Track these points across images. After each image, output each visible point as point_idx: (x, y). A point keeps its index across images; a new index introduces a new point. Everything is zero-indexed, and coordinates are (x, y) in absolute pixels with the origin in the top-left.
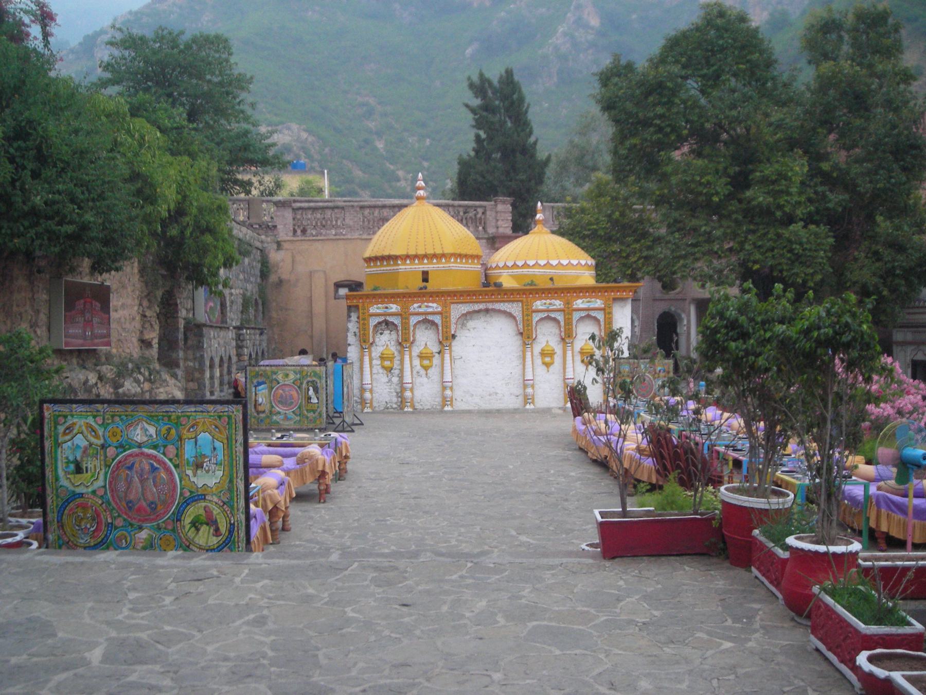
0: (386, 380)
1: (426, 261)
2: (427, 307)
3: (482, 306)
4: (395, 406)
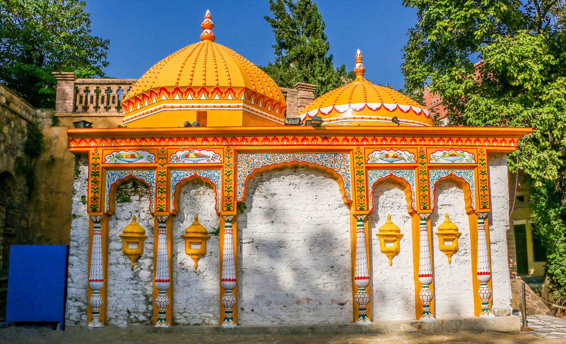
0: (129, 274)
1: (203, 97)
2: (198, 156)
3: (286, 158)
4: (142, 318)
